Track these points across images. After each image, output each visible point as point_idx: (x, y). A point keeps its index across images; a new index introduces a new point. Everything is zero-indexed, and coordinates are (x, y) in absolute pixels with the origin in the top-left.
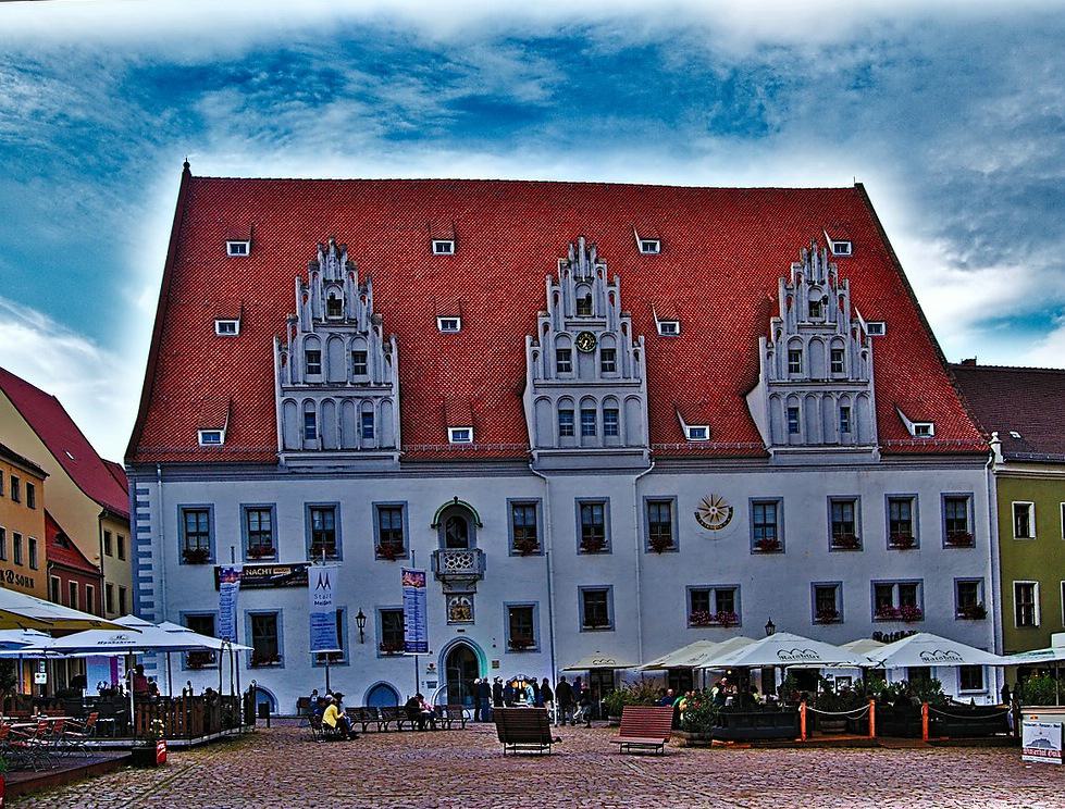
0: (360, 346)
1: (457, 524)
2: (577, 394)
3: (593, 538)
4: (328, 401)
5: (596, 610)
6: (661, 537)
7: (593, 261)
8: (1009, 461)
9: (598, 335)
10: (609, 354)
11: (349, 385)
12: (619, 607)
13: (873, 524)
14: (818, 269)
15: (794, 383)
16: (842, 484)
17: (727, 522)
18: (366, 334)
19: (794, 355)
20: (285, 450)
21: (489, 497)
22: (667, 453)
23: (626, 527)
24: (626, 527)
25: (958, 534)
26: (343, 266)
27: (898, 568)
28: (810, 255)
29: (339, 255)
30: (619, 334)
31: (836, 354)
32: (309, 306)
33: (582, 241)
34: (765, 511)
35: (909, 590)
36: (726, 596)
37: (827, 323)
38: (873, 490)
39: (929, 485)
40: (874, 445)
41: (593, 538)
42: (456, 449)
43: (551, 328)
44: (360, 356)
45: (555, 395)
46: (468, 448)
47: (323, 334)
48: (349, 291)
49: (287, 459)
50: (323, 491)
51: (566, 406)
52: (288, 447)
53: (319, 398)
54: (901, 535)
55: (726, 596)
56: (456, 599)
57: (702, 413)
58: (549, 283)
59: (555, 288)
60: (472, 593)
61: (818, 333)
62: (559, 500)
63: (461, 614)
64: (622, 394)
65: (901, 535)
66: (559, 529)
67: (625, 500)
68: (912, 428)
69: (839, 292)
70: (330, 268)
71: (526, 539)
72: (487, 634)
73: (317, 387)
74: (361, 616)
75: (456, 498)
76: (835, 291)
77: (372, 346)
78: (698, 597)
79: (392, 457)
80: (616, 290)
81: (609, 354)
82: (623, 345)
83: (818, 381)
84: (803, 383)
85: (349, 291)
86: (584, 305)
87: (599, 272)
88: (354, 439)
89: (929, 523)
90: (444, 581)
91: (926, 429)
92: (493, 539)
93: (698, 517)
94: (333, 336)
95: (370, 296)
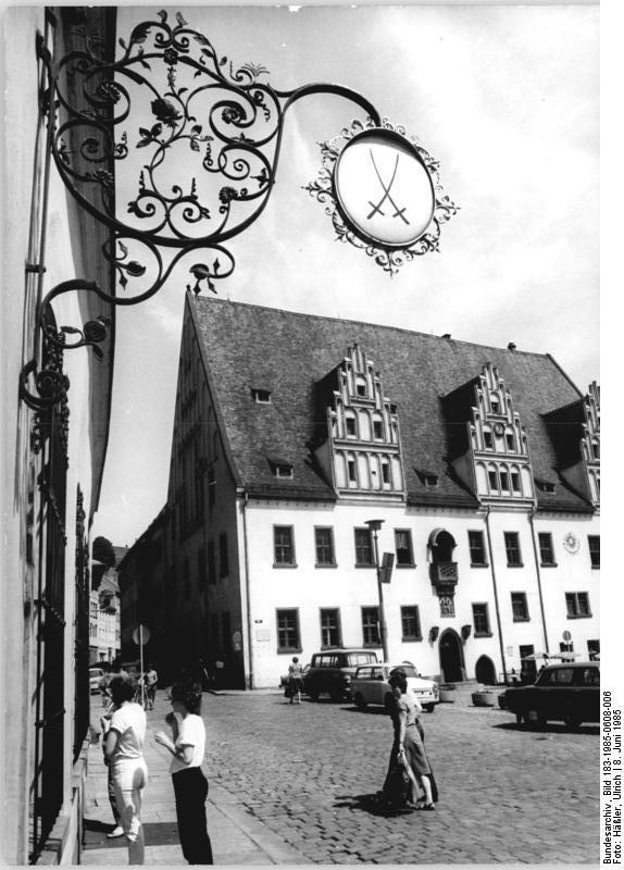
1: (442, 545)
3: (514, 559)
5: (519, 602)
10: (510, 439)
21: (458, 526)
22: (547, 508)
34: (594, 542)
41: (514, 559)
55: (583, 597)
63: (447, 611)
71: (479, 558)
92: (461, 554)
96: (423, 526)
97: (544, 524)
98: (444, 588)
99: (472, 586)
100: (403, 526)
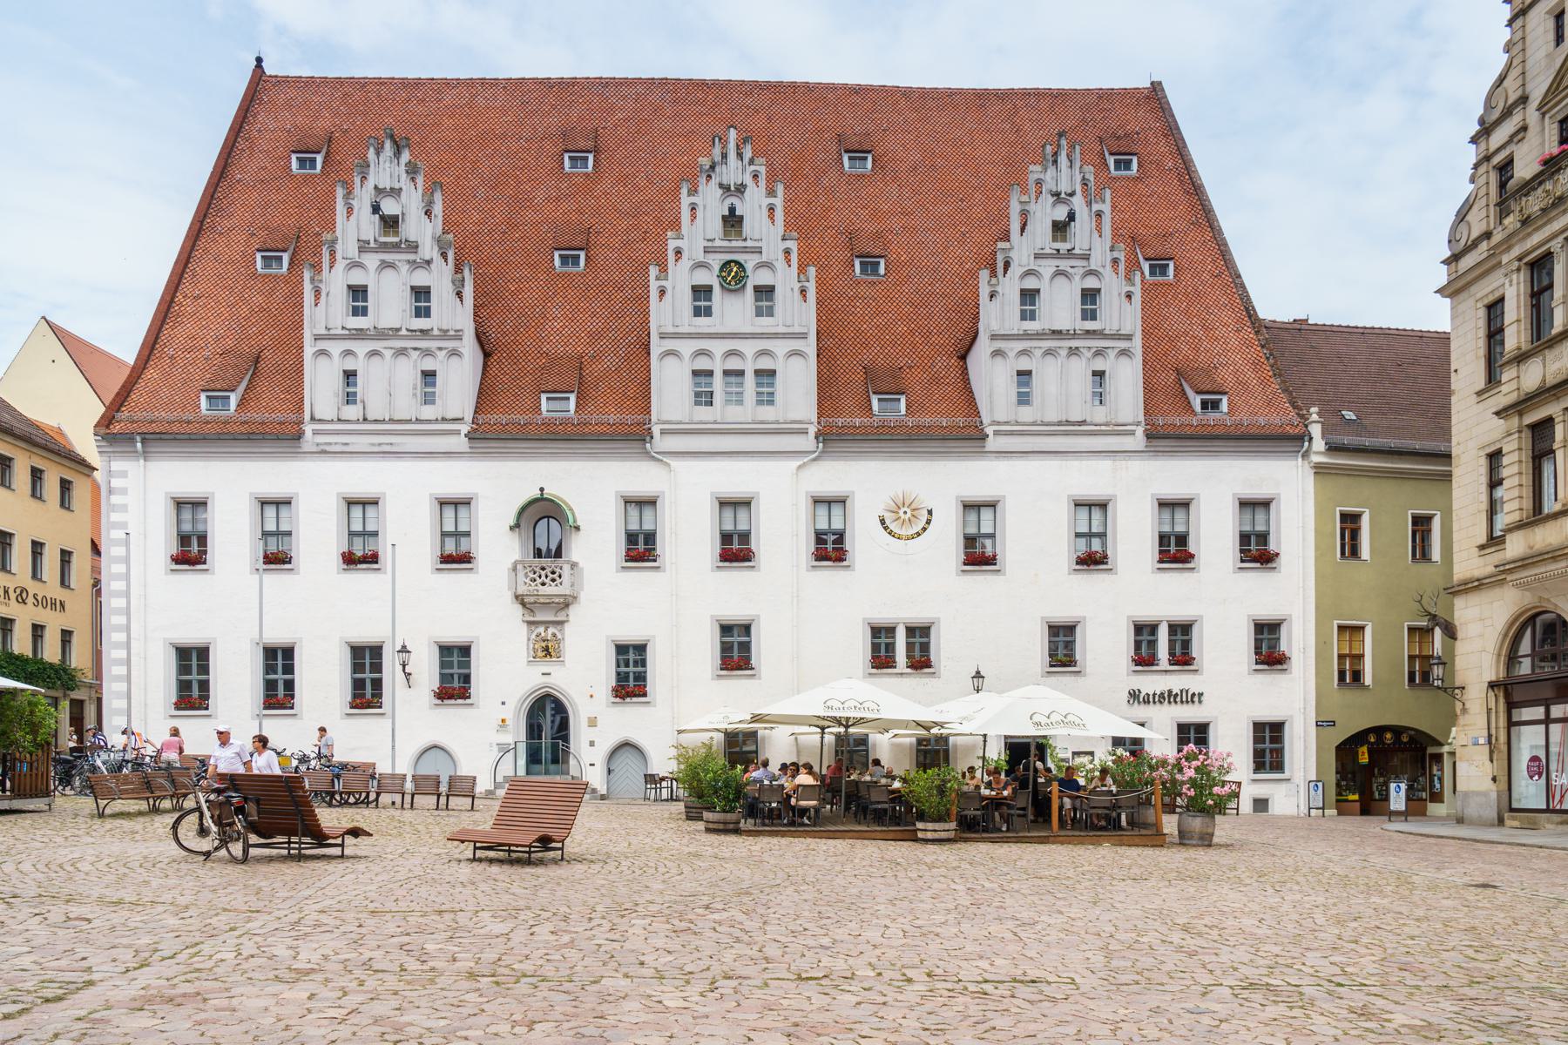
0: (421, 278)
2: (719, 348)
3: (736, 550)
4: (374, 353)
5: (736, 649)
6: (830, 549)
7: (746, 160)
8: (1332, 448)
9: (749, 267)
10: (764, 292)
11: (404, 332)
12: (764, 647)
13: (1134, 536)
14: (1065, 176)
15: (1026, 336)
16: (1092, 478)
17: (924, 529)
18: (428, 262)
19: (1029, 296)
20: (313, 419)
22: (838, 432)
23: (782, 533)
24: (782, 533)
25: (1256, 551)
26: (403, 168)
27: (1167, 595)
28: (1055, 154)
29: (398, 153)
30: (780, 264)
31: (1090, 296)
32: (354, 226)
33: (733, 133)
35: (1182, 631)
36: (920, 634)
37: (1077, 251)
38: (1137, 484)
39: (1216, 484)
40: (1138, 424)
41: (736, 550)
42: (547, 423)
43: (685, 255)
44: (421, 293)
45: (687, 348)
46: (565, 422)
47: (372, 261)
48: (409, 205)
49: (315, 433)
50: (361, 477)
51: (703, 363)
52: (317, 417)
53: (362, 348)
54: (1175, 551)
55: (920, 634)
56: (541, 629)
57: (897, 378)
58: (684, 191)
59: (693, 199)
60: (561, 623)
61: (1064, 264)
62: (688, 496)
63: (548, 651)
64: (780, 348)
65: (1175, 551)
66: (688, 534)
67: (782, 495)
68: (1196, 402)
69: (1095, 207)
70: (385, 170)
71: (640, 548)
72: (583, 679)
73: (359, 334)
74: (404, 650)
75: (542, 490)
76: (1089, 204)
77: (439, 278)
78: (881, 635)
79: (458, 432)
80: (778, 201)
81: (764, 292)
82: (785, 279)
83: (1060, 332)
84: (1039, 336)
85: (409, 205)
86: (733, 221)
87: (755, 177)
88: (407, 404)
89: (1215, 535)
90: (523, 604)
91: (1215, 405)
92: (595, 545)
93: (883, 522)
94: (385, 265)
95: (438, 209)
96: (501, 484)
97: (835, 475)
98: (545, 614)
99: (609, 603)
100: (454, 488)
